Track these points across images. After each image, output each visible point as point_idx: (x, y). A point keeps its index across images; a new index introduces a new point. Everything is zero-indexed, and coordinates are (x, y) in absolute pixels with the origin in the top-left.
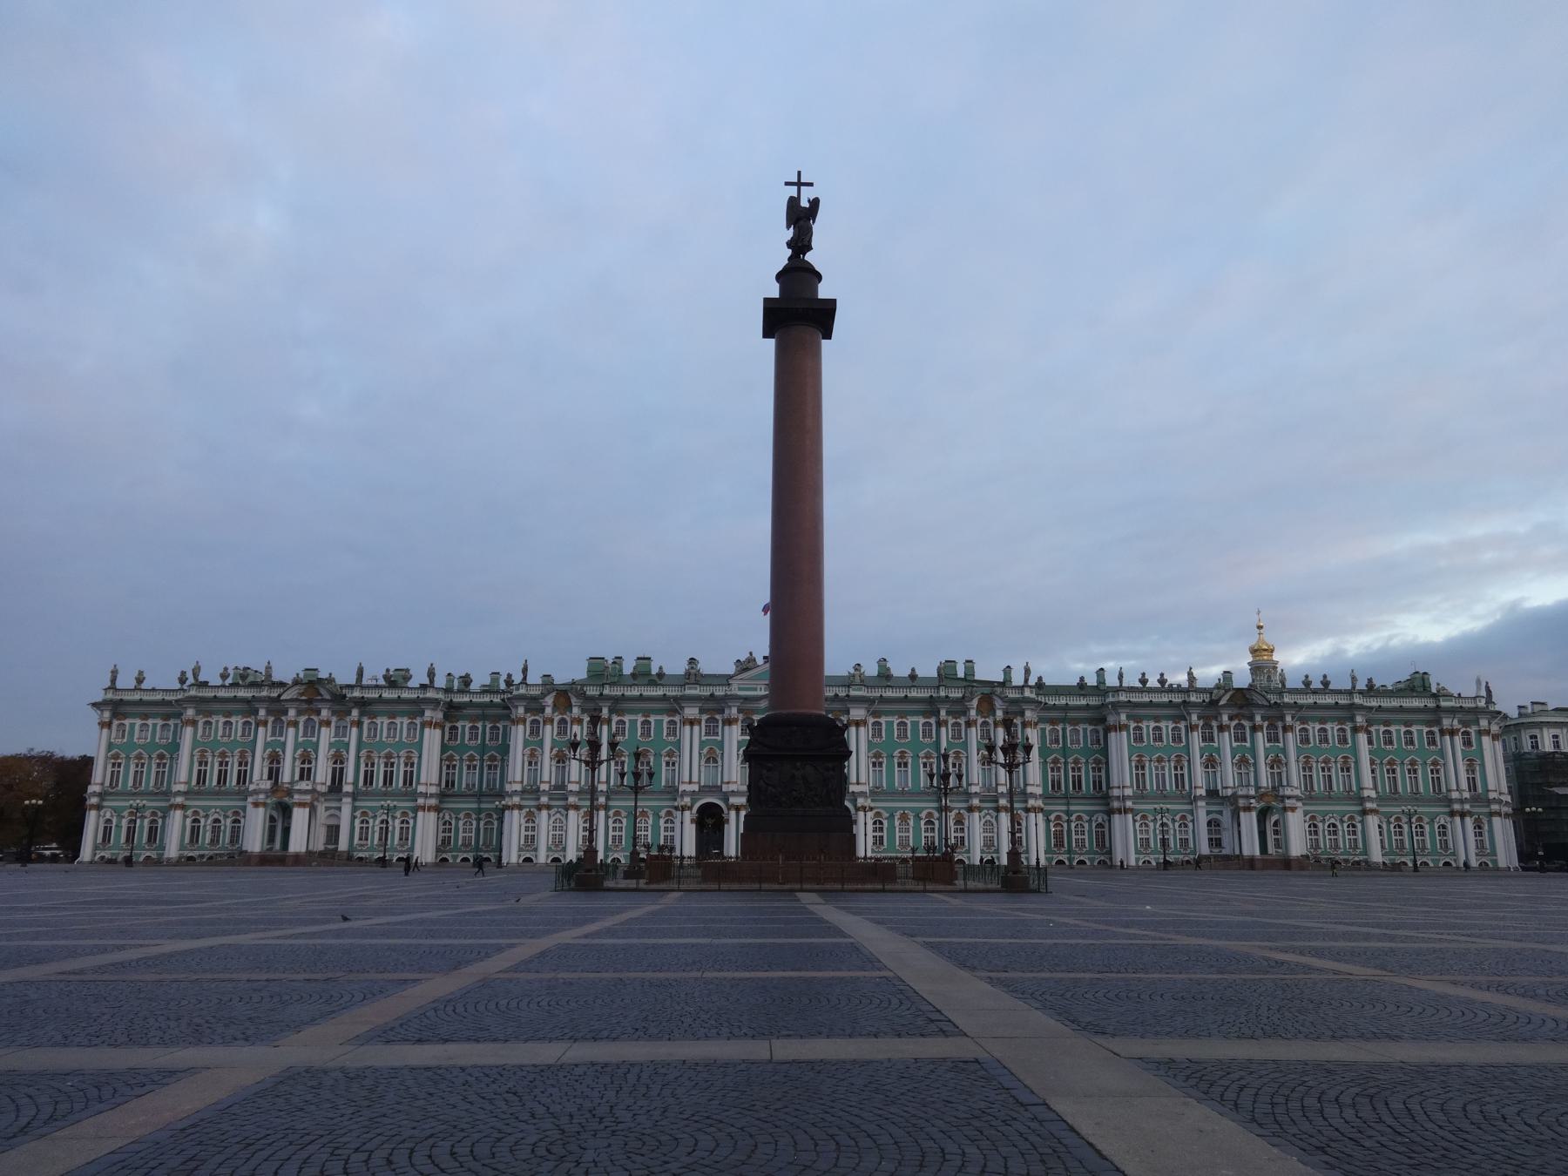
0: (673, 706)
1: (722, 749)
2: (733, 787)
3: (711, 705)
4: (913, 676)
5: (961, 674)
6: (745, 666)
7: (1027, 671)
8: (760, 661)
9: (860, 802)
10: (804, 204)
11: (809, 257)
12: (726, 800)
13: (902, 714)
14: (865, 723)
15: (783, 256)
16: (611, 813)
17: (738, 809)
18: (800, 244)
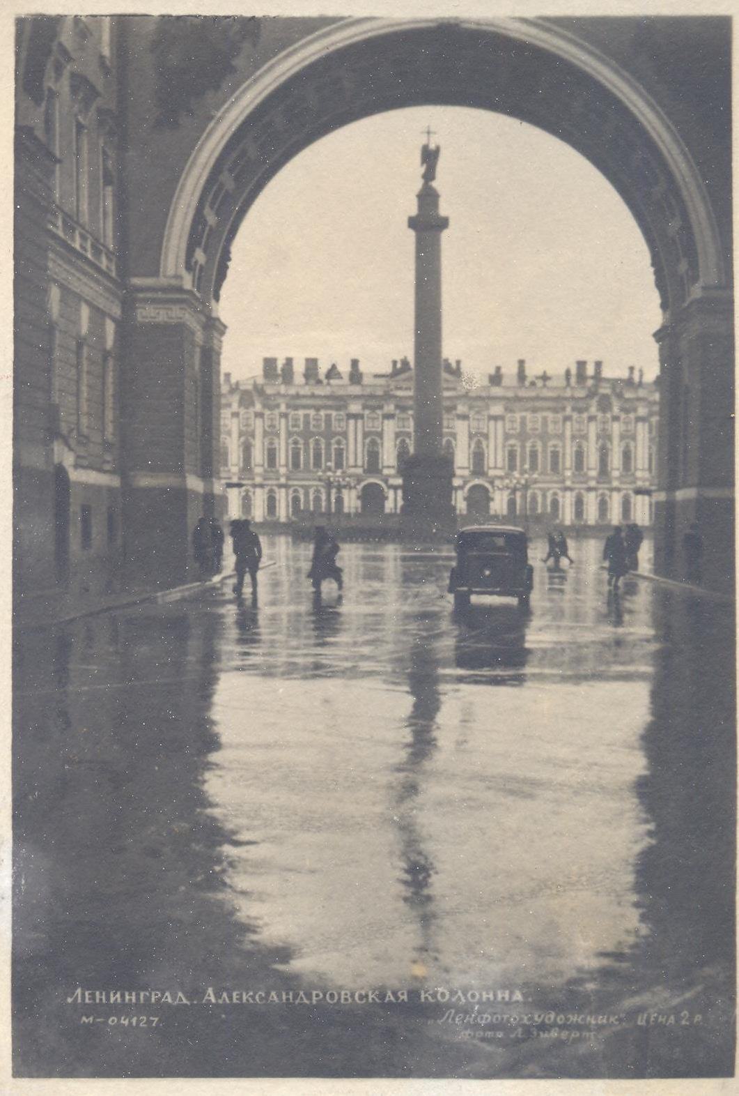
0: (339, 402)
1: (382, 438)
2: (392, 471)
3: (372, 403)
4: (545, 378)
5: (590, 370)
6: (400, 369)
7: (641, 376)
8: (412, 364)
9: (497, 483)
10: (432, 146)
11: (434, 184)
12: (386, 481)
13: (535, 410)
14: (502, 418)
15: (418, 184)
16: (291, 491)
17: (395, 488)
18: (429, 175)
